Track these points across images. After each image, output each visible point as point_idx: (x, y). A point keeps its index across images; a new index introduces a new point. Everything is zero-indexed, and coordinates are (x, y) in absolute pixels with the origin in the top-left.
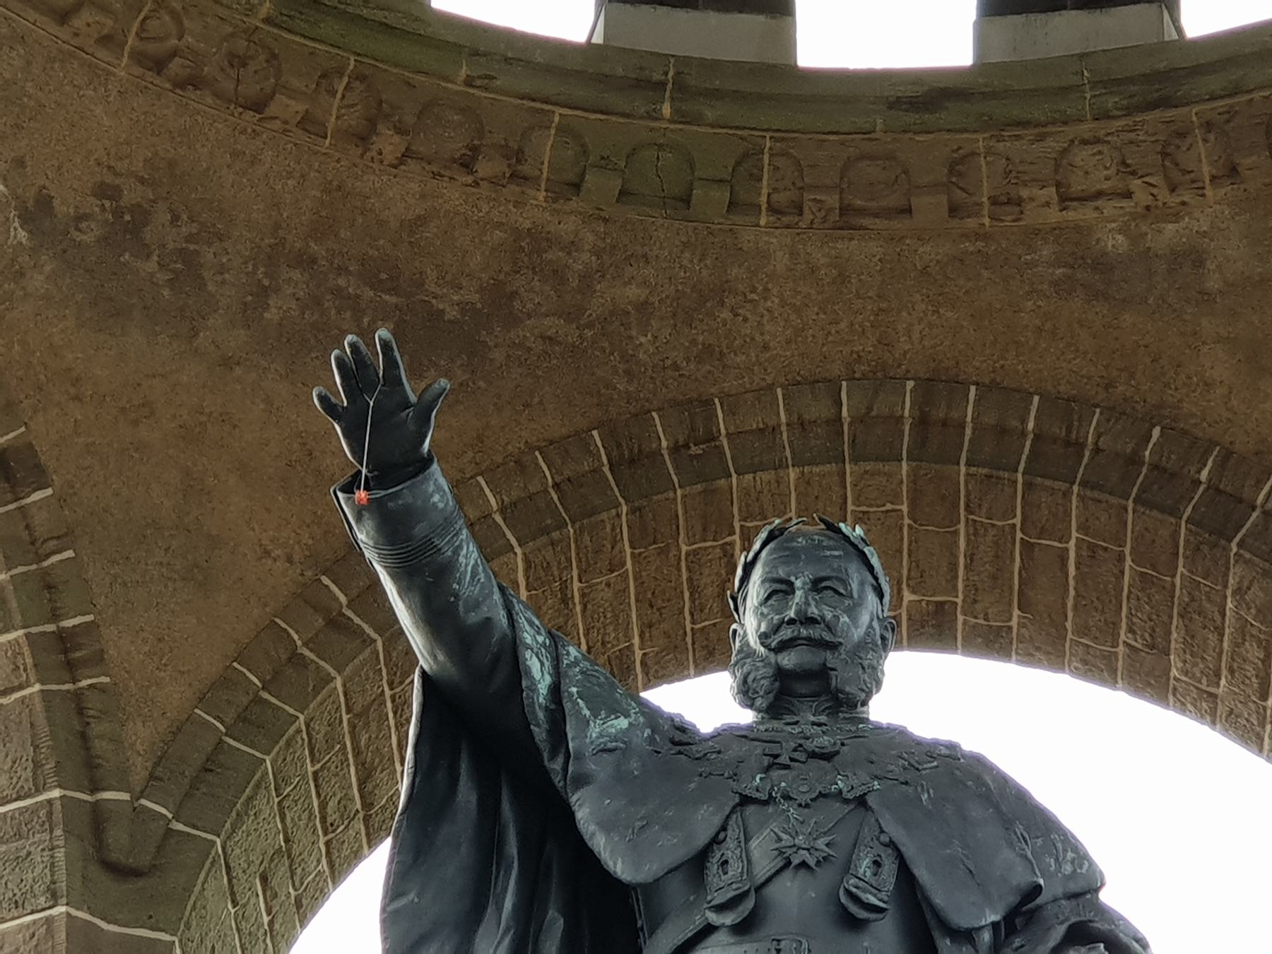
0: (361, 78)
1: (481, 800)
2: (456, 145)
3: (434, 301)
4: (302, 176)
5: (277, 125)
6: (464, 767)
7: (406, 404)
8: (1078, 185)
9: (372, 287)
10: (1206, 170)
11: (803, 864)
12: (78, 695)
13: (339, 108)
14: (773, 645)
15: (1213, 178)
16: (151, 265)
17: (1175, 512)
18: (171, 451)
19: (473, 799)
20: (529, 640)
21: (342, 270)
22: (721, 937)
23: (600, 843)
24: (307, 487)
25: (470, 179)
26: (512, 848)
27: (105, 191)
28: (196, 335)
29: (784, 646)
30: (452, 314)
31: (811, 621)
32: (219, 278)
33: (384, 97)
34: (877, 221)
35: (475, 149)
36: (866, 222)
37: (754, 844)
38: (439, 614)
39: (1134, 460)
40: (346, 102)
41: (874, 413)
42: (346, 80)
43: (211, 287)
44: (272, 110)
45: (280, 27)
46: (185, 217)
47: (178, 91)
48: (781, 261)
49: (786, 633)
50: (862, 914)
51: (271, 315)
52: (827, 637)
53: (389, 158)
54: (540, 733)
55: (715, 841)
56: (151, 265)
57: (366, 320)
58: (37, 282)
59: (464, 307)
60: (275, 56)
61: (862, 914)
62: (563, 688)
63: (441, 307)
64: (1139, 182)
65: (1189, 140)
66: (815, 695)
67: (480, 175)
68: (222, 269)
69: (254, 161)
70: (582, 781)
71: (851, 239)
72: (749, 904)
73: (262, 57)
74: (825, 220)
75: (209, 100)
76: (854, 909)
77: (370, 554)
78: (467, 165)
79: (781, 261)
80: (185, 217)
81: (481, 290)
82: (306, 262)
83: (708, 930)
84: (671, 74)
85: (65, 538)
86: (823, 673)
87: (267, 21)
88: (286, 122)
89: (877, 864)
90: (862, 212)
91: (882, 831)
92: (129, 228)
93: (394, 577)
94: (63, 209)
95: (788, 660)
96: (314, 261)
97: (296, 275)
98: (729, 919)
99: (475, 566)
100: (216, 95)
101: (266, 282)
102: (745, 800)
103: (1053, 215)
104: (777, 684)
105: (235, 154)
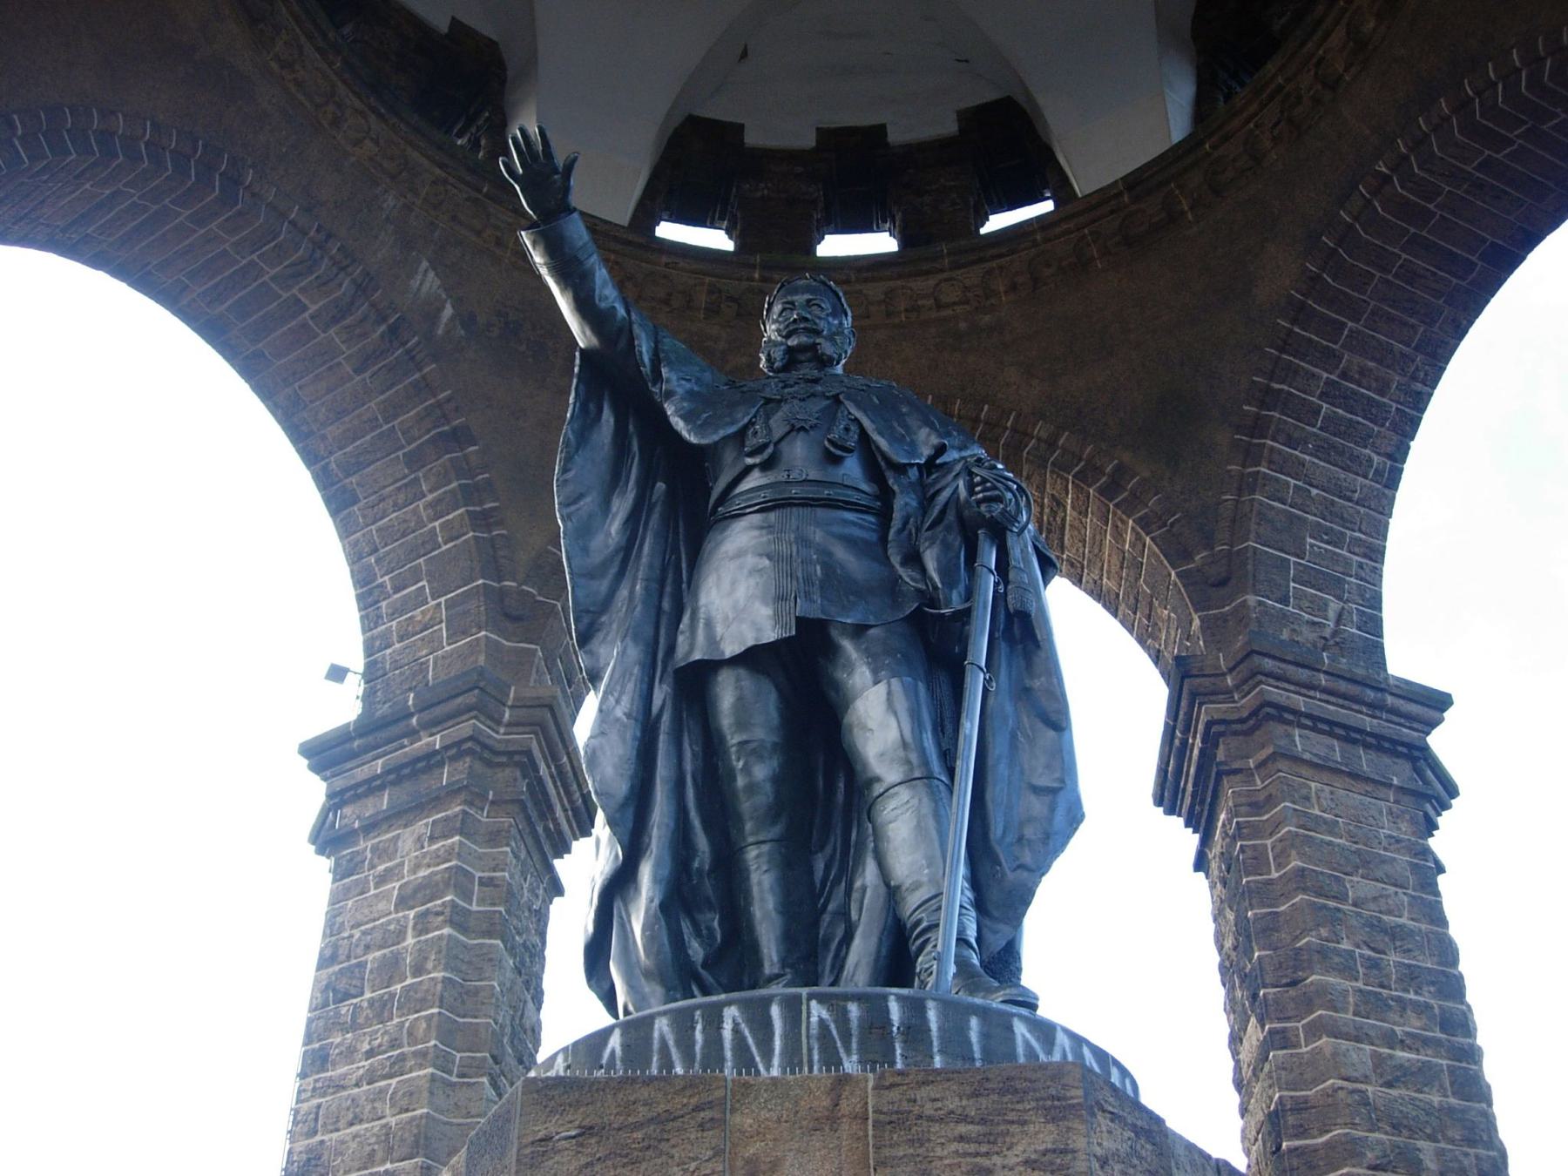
1: (617, 421)
7: (556, 171)
8: (944, 299)
10: (1002, 289)
11: (802, 428)
12: (492, 539)
16: (523, 348)
17: (997, 441)
19: (612, 420)
22: (756, 474)
23: (679, 424)
26: (635, 448)
29: (787, 337)
31: (806, 320)
35: (670, 294)
38: (584, 306)
39: (976, 420)
50: (839, 453)
54: (646, 369)
55: (751, 423)
56: (523, 348)
61: (839, 453)
70: (669, 395)
72: (770, 450)
77: (544, 271)
78: (666, 302)
83: (748, 470)
86: (814, 346)
89: (847, 429)
93: (558, 283)
95: (793, 342)
98: (757, 460)
102: (768, 401)
103: (934, 315)
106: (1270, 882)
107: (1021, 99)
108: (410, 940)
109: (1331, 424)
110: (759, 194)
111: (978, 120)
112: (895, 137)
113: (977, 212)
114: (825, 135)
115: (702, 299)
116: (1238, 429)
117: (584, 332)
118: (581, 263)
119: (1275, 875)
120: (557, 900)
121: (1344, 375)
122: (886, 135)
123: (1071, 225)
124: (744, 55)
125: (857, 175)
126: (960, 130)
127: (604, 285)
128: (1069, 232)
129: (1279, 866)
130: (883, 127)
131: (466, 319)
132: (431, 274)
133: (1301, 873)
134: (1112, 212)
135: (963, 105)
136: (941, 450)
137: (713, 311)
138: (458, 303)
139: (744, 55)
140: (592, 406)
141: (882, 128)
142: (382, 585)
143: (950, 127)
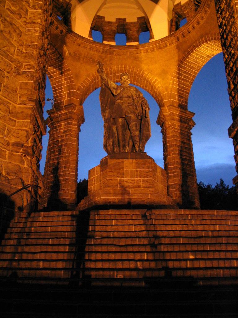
16: (77, 57)
27: (74, 52)
41: (234, 62)
48: (116, 58)
58: (70, 58)
79: (116, 58)
82: (86, 57)
85: (72, 75)
92: (75, 55)
94: (71, 53)
106: (169, 136)
108: (65, 138)
109: (185, 76)
112: (128, 21)
114: (117, 19)
115: (101, 51)
116: (172, 76)
119: (170, 135)
120: (80, 132)
121: (187, 70)
122: (126, 20)
129: (171, 134)
130: (125, 19)
131: (70, 54)
132: (65, 47)
133: (173, 135)
135: (138, 17)
137: (103, 52)
138: (69, 51)
142: (57, 89)
143: (136, 20)
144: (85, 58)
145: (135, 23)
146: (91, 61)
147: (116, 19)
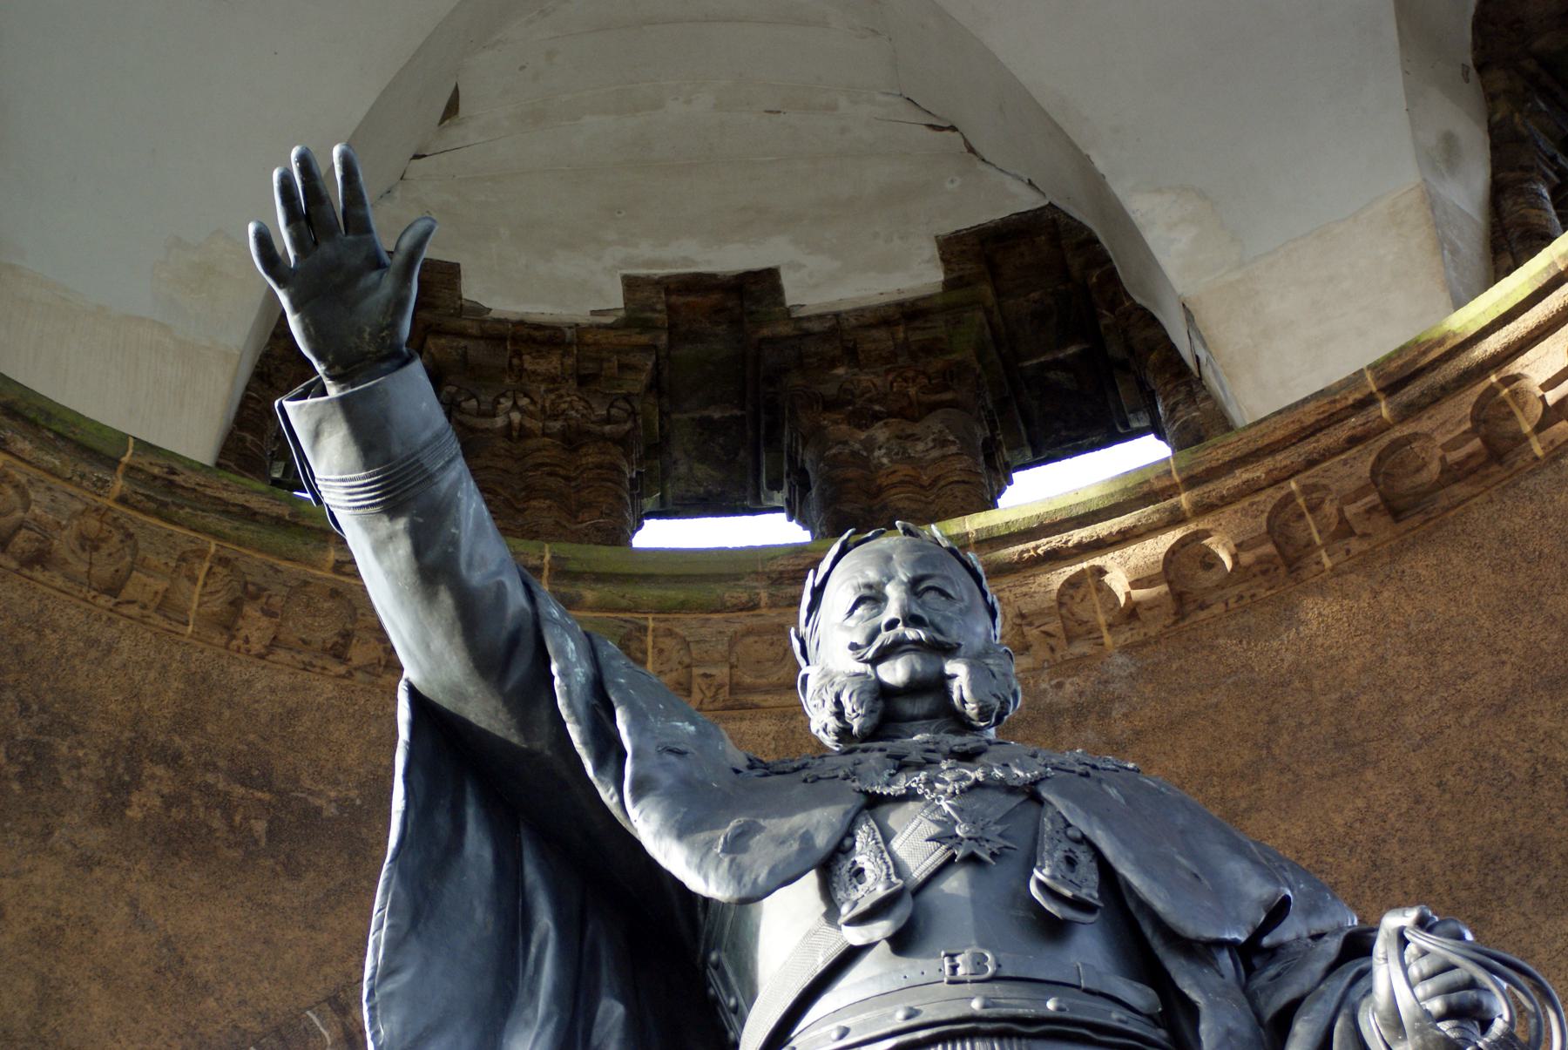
0: (224, 561)
2: (327, 633)
3: (310, 799)
4: (164, 666)
5: (134, 610)
6: (471, 813)
9: (243, 784)
10: (1102, 619)
13: (201, 595)
14: (870, 655)
15: (1110, 626)
18: (25, 957)
19: (487, 854)
20: (556, 613)
21: (210, 766)
24: (177, 995)
25: (342, 670)
28: (51, 833)
30: (331, 811)
32: (75, 773)
33: (249, 578)
34: (769, 697)
35: (347, 636)
36: (756, 698)
37: (896, 844)
40: (208, 589)
42: (207, 565)
43: (67, 782)
44: (130, 591)
45: (135, 508)
46: (35, 707)
47: (26, 572)
49: (885, 637)
51: (134, 813)
52: (940, 638)
53: (257, 647)
57: (238, 819)
59: (343, 803)
60: (130, 536)
62: (607, 677)
63: (318, 802)
64: (1035, 632)
65: (1082, 591)
66: (930, 716)
67: (356, 661)
68: (78, 764)
69: (110, 650)
71: (742, 719)
72: (903, 911)
73: (117, 537)
74: (714, 698)
75: (59, 582)
76: (1052, 908)
80: (35, 707)
81: (361, 785)
82: (173, 759)
84: (548, 557)
87: (122, 500)
88: (144, 607)
90: (751, 689)
91: (1069, 825)
95: (895, 672)
96: (178, 756)
97: (160, 771)
98: (880, 929)
99: (478, 513)
100: (68, 577)
101: (127, 778)
104: (880, 704)
105: (92, 643)
107: (1082, 213)
110: (500, 422)
111: (979, 253)
113: (990, 459)
117: (426, 646)
118: (430, 478)
122: (777, 290)
123: (1257, 472)
124: (452, 108)
125: (732, 384)
126: (949, 285)
127: (479, 526)
128: (1252, 489)
134: (1353, 441)
135: (948, 227)
136: (1278, 911)
139: (452, 108)
140: (442, 820)
141: (765, 282)
143: (920, 275)
144: (149, 768)
145: (910, 312)
146: (260, 827)
147: (631, 284)
